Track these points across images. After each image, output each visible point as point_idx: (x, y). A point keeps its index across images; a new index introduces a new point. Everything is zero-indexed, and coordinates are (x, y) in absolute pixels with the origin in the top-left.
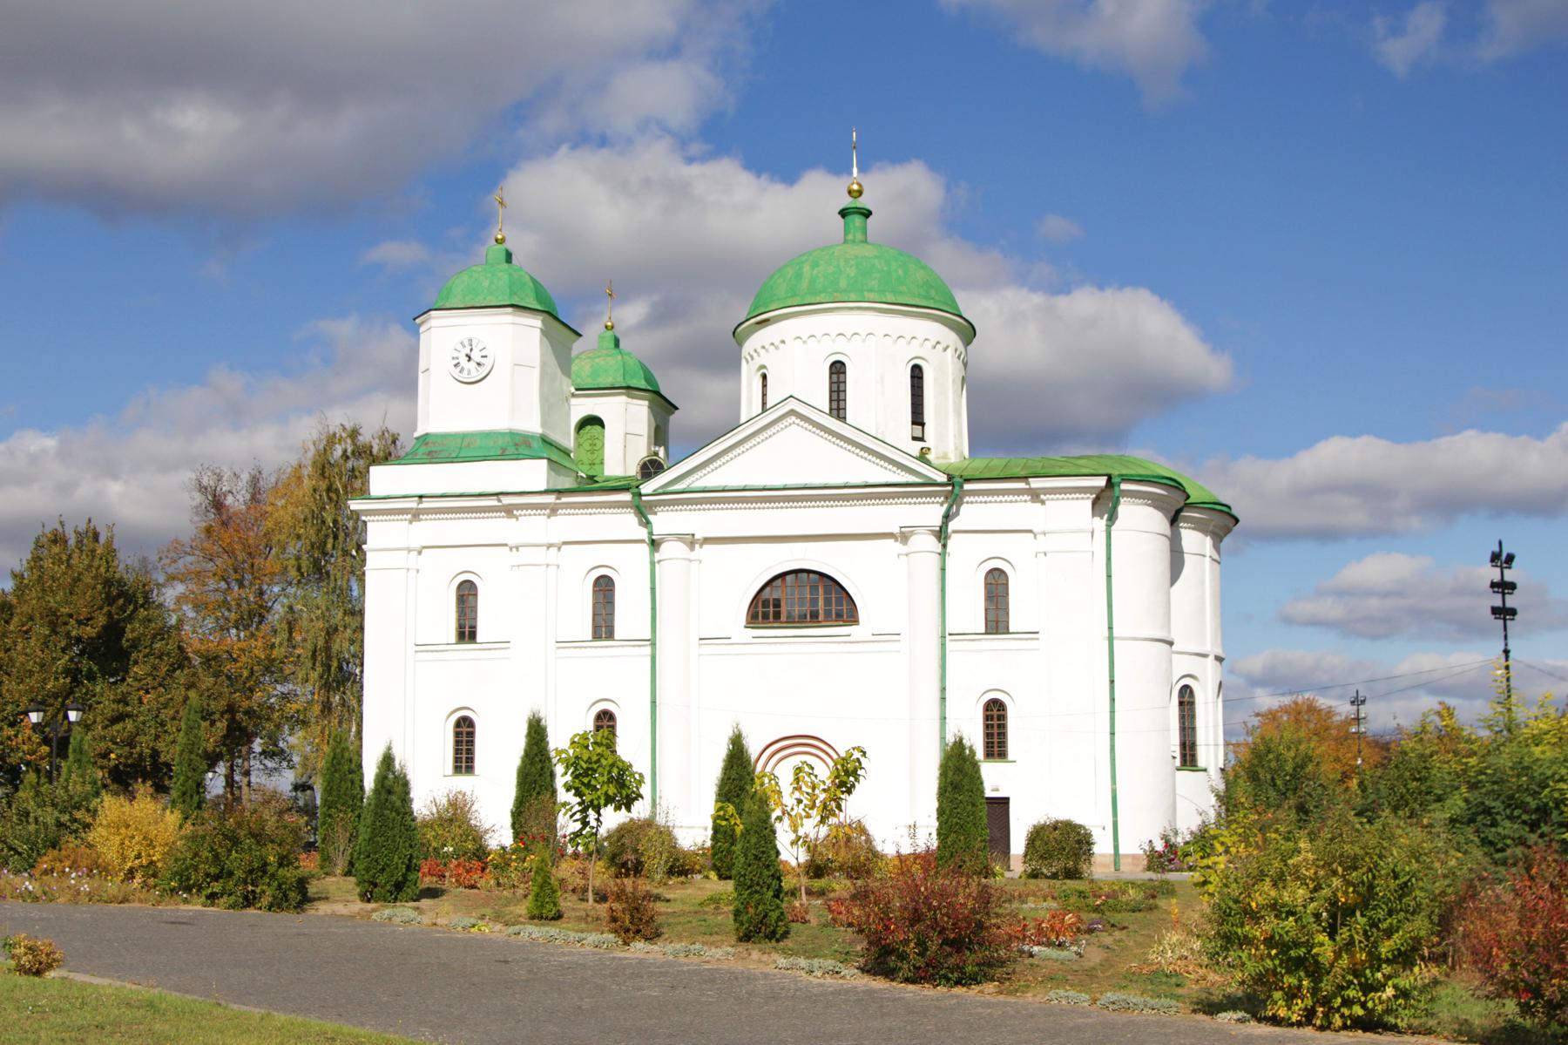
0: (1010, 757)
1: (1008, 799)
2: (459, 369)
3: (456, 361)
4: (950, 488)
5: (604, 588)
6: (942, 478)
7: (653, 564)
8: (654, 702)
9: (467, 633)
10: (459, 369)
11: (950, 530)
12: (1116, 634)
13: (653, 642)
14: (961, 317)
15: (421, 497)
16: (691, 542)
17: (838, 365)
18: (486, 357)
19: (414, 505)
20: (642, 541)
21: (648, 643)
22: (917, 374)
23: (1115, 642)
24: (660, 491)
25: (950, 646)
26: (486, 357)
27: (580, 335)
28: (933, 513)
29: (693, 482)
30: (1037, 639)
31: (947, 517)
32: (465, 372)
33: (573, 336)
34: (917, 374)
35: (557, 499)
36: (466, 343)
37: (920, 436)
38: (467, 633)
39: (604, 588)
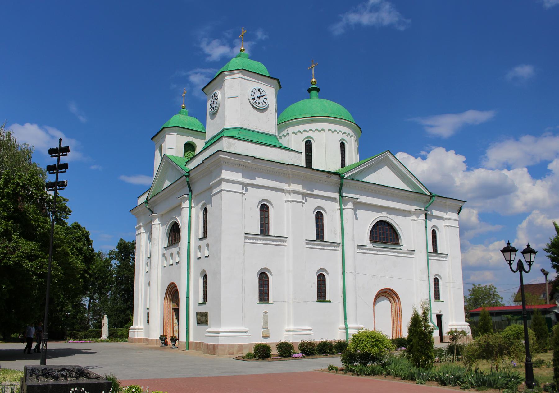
0: (441, 299)
2: (255, 101)
3: (253, 97)
4: (429, 198)
5: (319, 217)
6: (429, 194)
7: (341, 210)
8: (344, 271)
9: (264, 229)
10: (255, 101)
15: (255, 157)
18: (266, 99)
26: (266, 99)
30: (413, 258)
32: (257, 103)
36: (258, 90)
38: (264, 229)
39: (319, 217)
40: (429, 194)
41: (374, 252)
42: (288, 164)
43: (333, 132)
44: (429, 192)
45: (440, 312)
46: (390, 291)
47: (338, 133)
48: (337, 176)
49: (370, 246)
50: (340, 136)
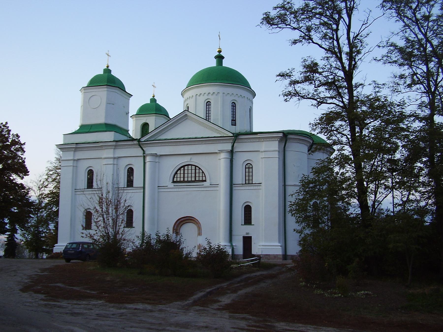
1: (251, 237)
4: (233, 138)
5: (130, 171)
6: (232, 135)
7: (145, 163)
11: (234, 151)
12: (287, 184)
13: (144, 188)
14: (251, 89)
15: (76, 144)
16: (155, 155)
17: (209, 102)
19: (74, 146)
20: (142, 156)
21: (143, 188)
22: (234, 105)
23: (287, 187)
24: (146, 140)
25: (234, 188)
27: (132, 96)
28: (228, 147)
29: (156, 138)
31: (233, 146)
33: (131, 96)
34: (234, 105)
35: (116, 143)
37: (235, 124)
40: (232, 135)
41: (176, 190)
42: (98, 142)
43: (199, 96)
44: (231, 133)
45: (247, 234)
46: (184, 219)
47: (203, 95)
48: (136, 141)
49: (172, 185)
50: (206, 97)
